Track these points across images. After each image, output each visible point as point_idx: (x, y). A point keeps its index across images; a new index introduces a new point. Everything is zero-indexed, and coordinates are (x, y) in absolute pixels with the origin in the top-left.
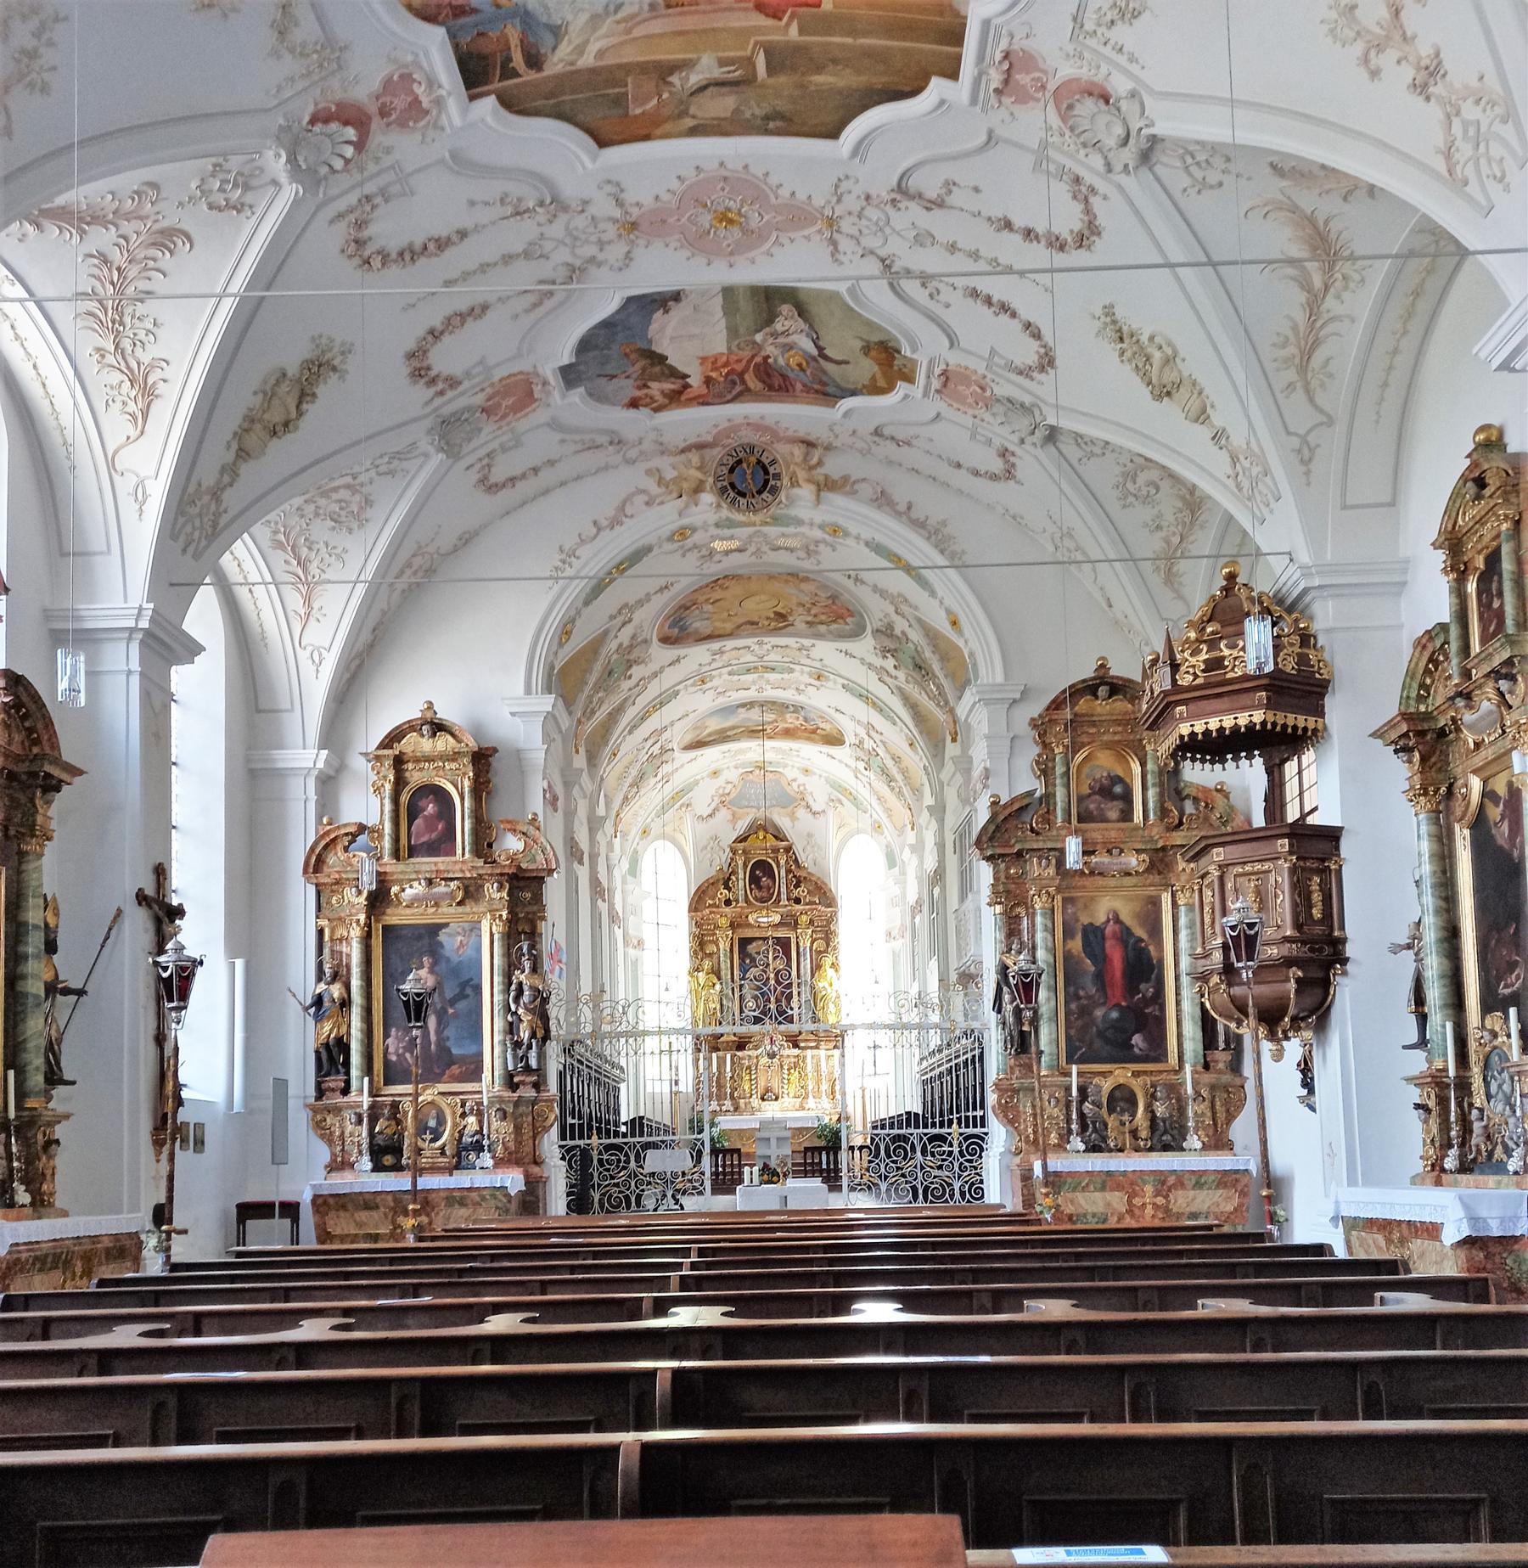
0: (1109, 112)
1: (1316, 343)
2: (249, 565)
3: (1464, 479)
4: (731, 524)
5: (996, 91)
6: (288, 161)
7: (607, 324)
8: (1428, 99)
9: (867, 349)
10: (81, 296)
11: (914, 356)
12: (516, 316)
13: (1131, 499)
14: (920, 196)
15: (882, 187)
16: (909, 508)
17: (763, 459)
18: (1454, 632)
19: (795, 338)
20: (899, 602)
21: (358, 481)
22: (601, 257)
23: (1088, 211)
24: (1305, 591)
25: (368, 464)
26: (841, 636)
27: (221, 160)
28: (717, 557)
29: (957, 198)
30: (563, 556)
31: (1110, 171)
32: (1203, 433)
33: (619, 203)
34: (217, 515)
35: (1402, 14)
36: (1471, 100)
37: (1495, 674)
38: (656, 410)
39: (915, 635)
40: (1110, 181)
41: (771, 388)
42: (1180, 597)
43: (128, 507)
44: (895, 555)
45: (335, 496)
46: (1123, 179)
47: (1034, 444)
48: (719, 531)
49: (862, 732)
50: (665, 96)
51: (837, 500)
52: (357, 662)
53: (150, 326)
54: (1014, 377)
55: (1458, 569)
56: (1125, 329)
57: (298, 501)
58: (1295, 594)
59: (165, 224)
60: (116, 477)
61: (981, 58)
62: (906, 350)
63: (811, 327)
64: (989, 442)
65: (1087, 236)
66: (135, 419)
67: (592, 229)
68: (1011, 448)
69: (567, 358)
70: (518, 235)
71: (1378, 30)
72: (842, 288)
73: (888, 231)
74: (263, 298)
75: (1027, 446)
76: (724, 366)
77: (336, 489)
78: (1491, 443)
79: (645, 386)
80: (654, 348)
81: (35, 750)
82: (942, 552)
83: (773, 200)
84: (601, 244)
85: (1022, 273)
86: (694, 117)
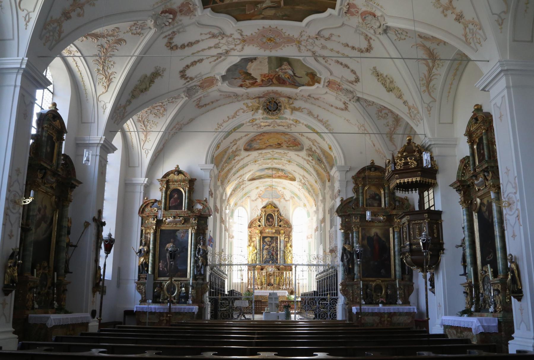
0: (375, 19)
1: (431, 80)
2: (131, 127)
3: (472, 118)
4: (266, 118)
5: (346, 13)
6: (154, 23)
7: (235, 65)
8: (460, 22)
9: (307, 74)
10: (96, 55)
11: (321, 77)
12: (210, 63)
13: (380, 117)
14: (324, 37)
15: (313, 34)
16: (318, 116)
18: (471, 159)
19: (287, 70)
20: (313, 141)
21: (163, 104)
22: (235, 48)
23: (369, 43)
24: (430, 145)
25: (166, 100)
26: (296, 150)
27: (136, 22)
28: (262, 127)
29: (333, 38)
30: (219, 126)
31: (375, 34)
32: (400, 102)
33: (241, 35)
34: (124, 113)
35: (452, 2)
36: (471, 24)
37: (484, 171)
38: (247, 88)
40: (375, 36)
41: (280, 83)
42: (394, 145)
43: (101, 110)
44: (314, 129)
45: (156, 108)
46: (379, 36)
47: (354, 101)
49: (301, 178)
50: (256, 9)
52: (158, 153)
53: (112, 63)
54: (348, 83)
55: (471, 142)
56: (379, 73)
57: (146, 109)
58: (427, 146)
59: (120, 37)
60: (99, 103)
61: (341, 4)
62: (318, 75)
63: (292, 68)
65: (369, 50)
66: (105, 87)
67: (233, 41)
68: (347, 102)
69: (224, 73)
70: (213, 42)
71: (446, 5)
72: (301, 58)
73: (314, 45)
74: (143, 57)
75: (352, 101)
76: (267, 77)
77: (157, 106)
78: (478, 109)
79: (245, 81)
80: (248, 72)
81: (69, 176)
82: (327, 129)
83: (283, 36)
84: (236, 45)
85: (351, 58)
86: (263, 15)
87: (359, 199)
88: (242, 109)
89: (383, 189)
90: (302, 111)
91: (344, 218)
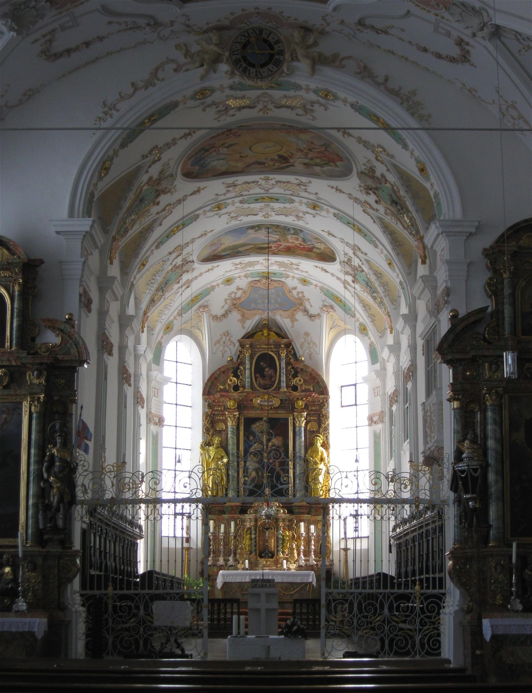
4: (241, 87)
16: (386, 80)
17: (270, 39)
26: (331, 176)
28: (231, 112)
30: (106, 109)
39: (392, 178)
44: (375, 115)
47: (483, 38)
48: (233, 92)
49: (350, 252)
51: (329, 72)
64: (448, 34)
68: (466, 39)
75: (478, 39)
82: (413, 115)
87: (503, 312)
88: (172, 61)
90: (344, 67)
91: (460, 368)
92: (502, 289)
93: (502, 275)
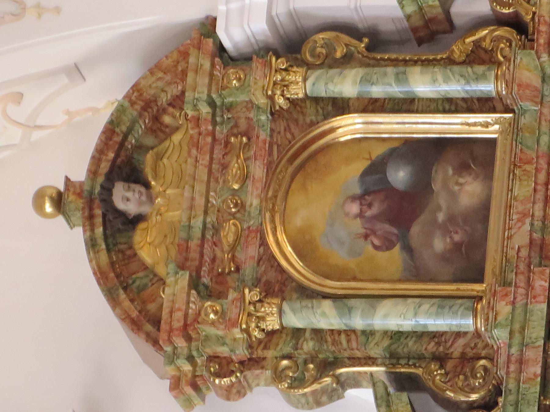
89: (327, 117)
92: (317, 333)
93: (271, 334)
